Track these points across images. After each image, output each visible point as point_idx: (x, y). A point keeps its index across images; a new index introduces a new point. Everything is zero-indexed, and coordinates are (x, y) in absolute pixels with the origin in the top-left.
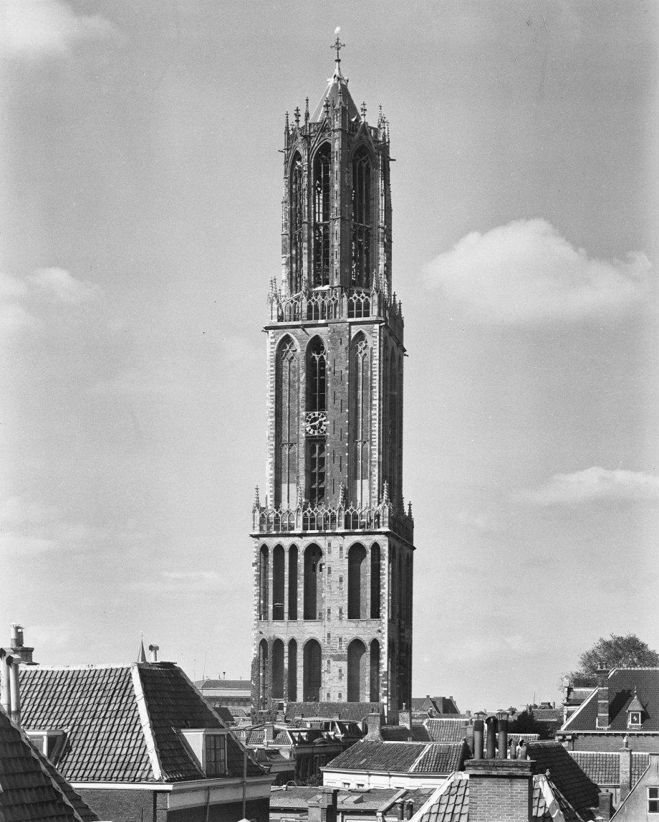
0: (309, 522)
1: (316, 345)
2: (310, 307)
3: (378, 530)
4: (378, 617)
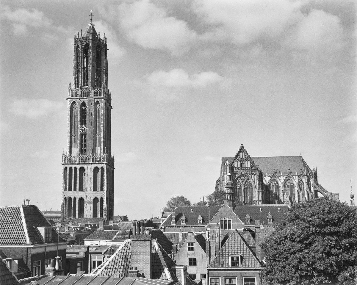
0: (81, 160)
1: (83, 104)
2: (81, 93)
3: (103, 163)
4: (103, 190)
